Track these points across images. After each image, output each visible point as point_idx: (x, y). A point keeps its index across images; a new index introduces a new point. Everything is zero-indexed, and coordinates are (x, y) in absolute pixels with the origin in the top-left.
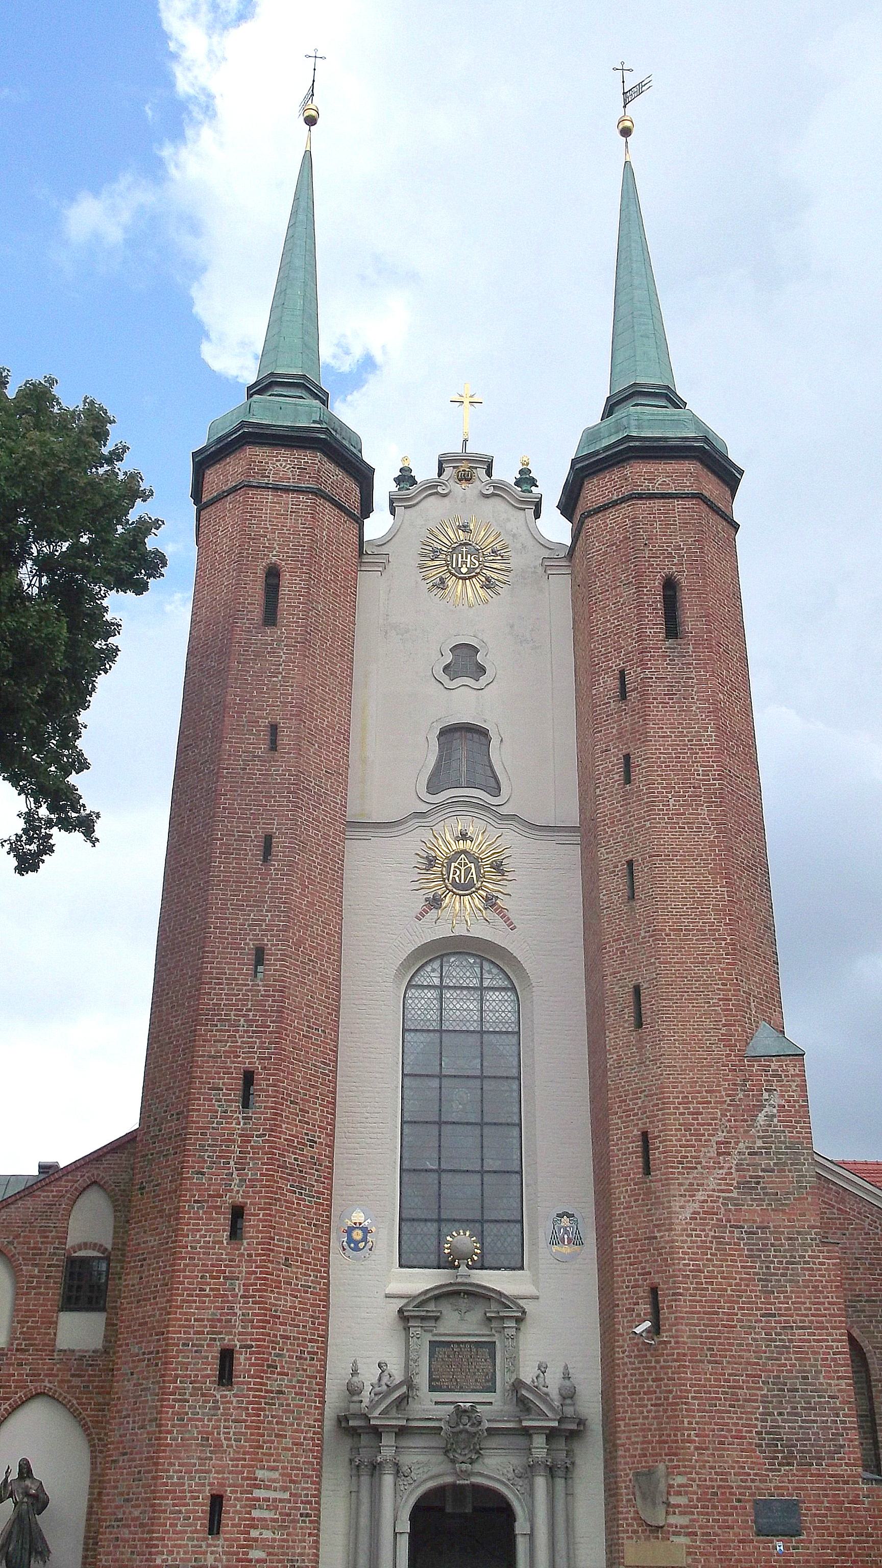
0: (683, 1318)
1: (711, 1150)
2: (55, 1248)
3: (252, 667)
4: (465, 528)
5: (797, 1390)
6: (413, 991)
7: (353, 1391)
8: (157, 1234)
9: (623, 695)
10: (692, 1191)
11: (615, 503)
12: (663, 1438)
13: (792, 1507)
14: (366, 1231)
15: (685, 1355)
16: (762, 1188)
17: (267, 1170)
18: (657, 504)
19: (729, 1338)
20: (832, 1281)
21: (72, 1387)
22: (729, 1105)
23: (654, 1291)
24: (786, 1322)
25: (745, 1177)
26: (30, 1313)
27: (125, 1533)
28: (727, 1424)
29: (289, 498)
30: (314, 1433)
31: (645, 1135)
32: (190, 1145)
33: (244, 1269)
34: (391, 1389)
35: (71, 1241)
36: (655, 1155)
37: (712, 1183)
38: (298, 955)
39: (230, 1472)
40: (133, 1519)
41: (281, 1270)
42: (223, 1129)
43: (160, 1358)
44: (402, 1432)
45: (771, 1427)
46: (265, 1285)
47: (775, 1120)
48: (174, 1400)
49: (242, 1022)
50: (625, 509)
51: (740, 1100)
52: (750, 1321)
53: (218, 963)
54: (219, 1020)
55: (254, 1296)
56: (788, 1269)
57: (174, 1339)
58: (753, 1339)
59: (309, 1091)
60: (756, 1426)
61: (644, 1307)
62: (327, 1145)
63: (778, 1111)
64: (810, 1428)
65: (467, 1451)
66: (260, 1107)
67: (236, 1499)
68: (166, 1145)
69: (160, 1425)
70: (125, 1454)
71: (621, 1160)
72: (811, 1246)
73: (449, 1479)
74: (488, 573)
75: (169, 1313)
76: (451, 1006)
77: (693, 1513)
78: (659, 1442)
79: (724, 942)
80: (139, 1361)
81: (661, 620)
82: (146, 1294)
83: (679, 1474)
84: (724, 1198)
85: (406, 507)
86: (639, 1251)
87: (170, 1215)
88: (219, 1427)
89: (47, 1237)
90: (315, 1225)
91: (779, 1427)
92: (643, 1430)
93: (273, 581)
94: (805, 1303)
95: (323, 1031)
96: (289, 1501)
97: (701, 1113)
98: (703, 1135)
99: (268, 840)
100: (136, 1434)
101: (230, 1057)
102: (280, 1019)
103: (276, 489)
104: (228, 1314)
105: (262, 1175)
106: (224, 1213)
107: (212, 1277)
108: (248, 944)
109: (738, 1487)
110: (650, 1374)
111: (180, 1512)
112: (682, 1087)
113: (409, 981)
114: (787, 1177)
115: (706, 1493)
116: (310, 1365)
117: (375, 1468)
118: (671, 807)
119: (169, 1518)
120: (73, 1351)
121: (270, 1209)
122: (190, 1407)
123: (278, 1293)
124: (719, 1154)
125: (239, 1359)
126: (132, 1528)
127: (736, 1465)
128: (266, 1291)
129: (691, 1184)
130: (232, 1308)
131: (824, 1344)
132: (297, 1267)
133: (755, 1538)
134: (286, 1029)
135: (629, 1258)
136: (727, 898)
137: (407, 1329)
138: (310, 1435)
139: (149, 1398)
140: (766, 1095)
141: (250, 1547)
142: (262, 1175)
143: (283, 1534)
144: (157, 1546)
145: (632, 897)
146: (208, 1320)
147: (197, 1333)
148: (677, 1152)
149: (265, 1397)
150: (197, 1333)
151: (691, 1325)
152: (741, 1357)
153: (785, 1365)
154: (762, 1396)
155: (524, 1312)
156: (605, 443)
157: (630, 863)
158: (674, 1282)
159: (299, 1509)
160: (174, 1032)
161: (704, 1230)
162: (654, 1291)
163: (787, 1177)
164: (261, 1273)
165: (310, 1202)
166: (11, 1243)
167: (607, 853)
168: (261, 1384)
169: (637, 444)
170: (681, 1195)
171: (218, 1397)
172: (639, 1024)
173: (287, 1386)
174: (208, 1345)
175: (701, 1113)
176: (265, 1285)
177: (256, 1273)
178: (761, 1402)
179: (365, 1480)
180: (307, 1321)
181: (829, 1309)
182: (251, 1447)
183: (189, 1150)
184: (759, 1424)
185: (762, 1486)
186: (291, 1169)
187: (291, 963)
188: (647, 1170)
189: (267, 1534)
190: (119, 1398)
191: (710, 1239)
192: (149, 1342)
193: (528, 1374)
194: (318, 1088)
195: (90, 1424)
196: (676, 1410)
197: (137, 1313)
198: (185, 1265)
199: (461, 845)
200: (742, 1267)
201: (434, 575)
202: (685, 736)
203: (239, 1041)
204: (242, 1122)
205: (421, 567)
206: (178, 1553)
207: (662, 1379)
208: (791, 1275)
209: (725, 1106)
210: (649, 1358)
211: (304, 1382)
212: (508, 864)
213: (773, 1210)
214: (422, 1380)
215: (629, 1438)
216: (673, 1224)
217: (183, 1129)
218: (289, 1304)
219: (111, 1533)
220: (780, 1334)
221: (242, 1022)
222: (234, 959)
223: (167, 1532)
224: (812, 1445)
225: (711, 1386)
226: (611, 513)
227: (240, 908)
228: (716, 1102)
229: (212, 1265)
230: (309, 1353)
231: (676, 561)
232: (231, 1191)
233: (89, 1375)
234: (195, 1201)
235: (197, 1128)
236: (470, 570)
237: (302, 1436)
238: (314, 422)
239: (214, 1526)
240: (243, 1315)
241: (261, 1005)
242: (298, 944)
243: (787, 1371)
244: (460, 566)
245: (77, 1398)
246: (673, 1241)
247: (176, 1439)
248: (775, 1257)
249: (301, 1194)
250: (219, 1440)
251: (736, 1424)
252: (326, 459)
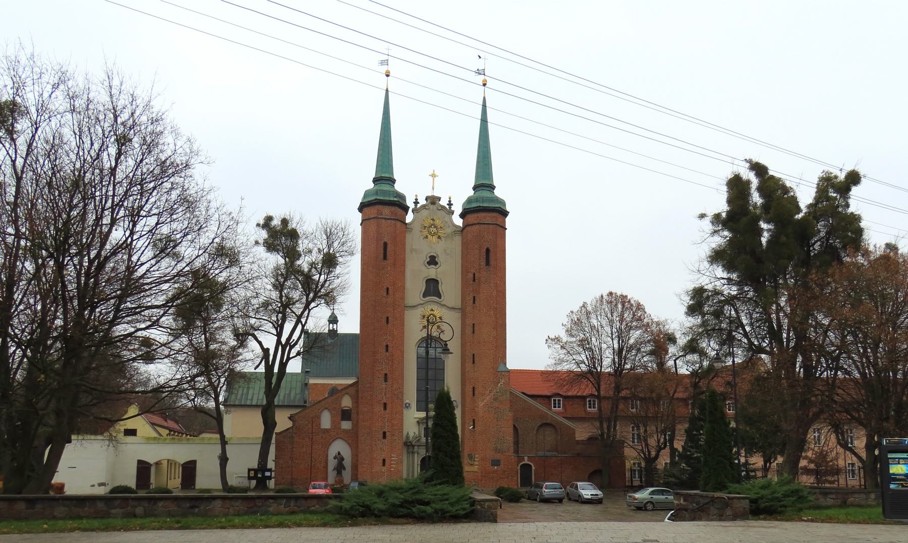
4: (433, 220)
7: (408, 437)
9: (474, 280)
10: (483, 400)
13: (499, 461)
14: (409, 404)
18: (486, 226)
23: (474, 420)
29: (389, 221)
31: (474, 388)
34: (416, 438)
36: (476, 392)
44: (418, 446)
50: (477, 226)
61: (472, 423)
99: (388, 318)
103: (385, 219)
117: (413, 453)
137: (419, 425)
145: (474, 332)
157: (474, 324)
162: (474, 420)
172: (474, 363)
179: (411, 455)
188: (474, 395)
199: (432, 312)
205: (421, 231)
236: (434, 233)
238: (395, 197)
239: (384, 465)
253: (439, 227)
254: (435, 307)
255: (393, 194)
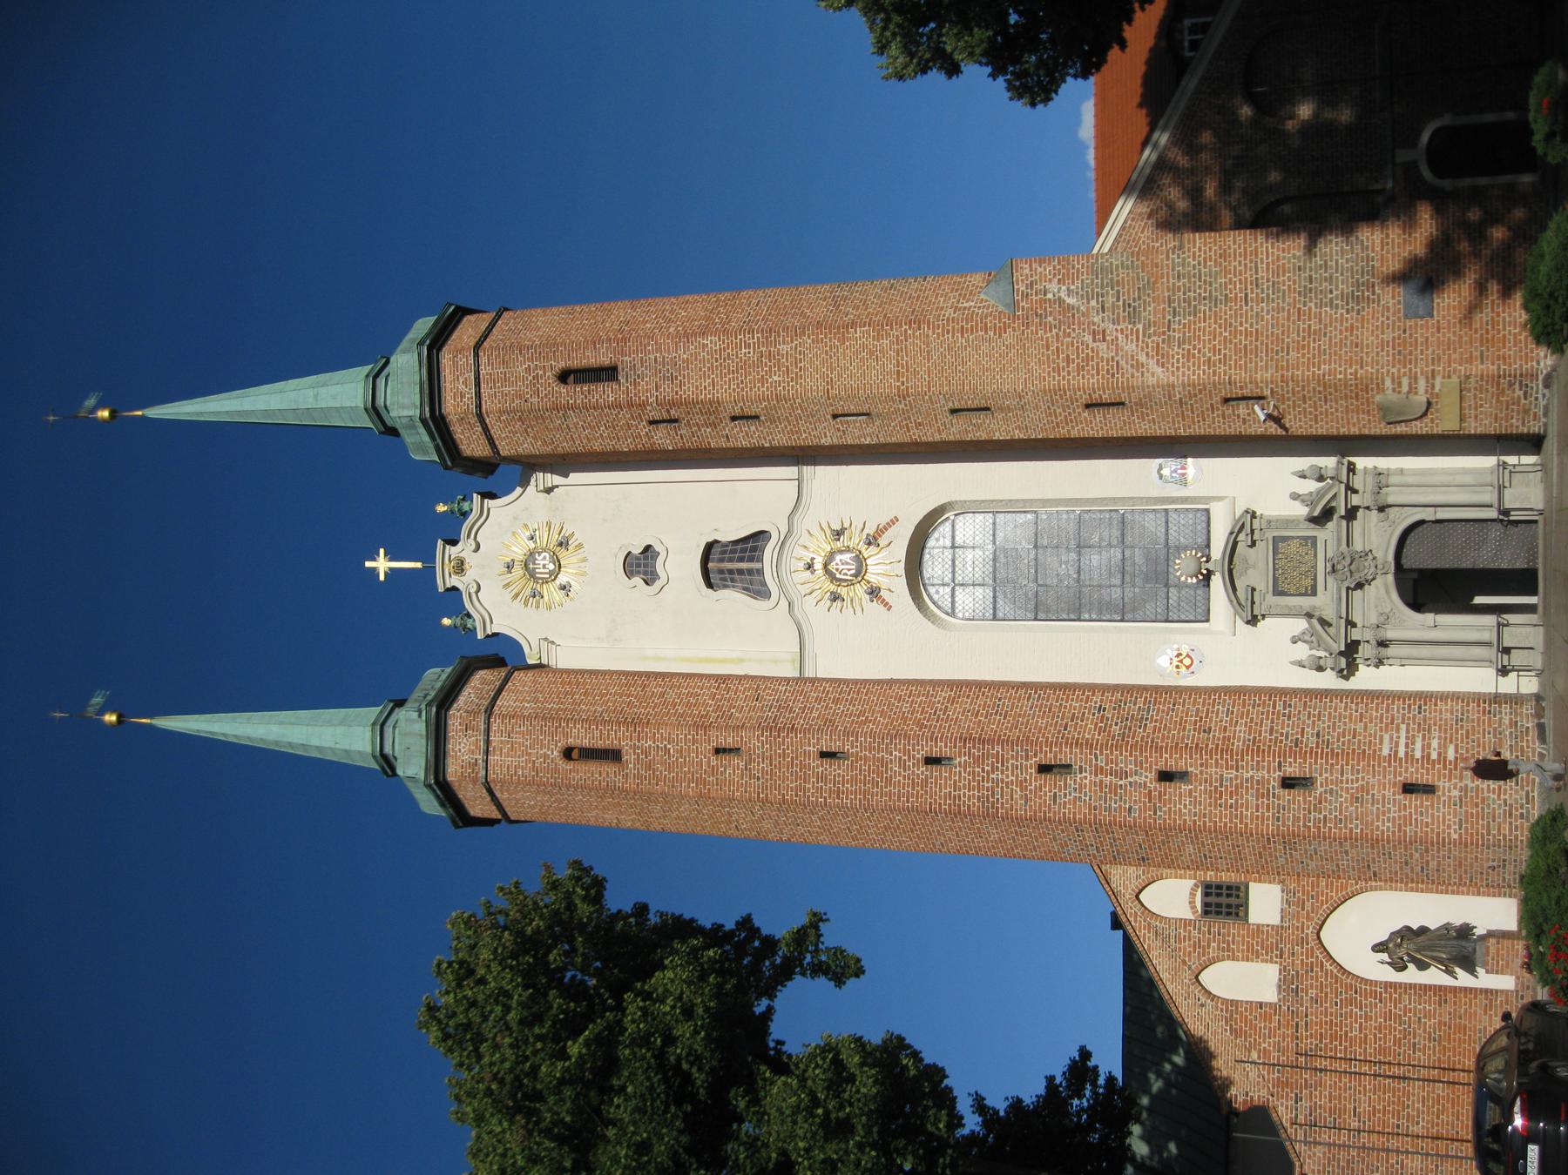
0: (1251, 377)
1: (1101, 347)
2: (1194, 929)
3: (661, 772)
5: (1310, 276)
6: (957, 611)
8: (1183, 845)
10: (1138, 366)
11: (486, 430)
12: (1354, 395)
15: (1282, 376)
16: (1134, 300)
17: (1126, 751)
19: (1267, 336)
20: (1215, 240)
21: (1313, 908)
22: (1060, 330)
23: (1226, 400)
24: (1252, 284)
25: (1124, 317)
26: (1250, 949)
27: (1432, 865)
28: (1341, 340)
30: (1352, 703)
31: (1088, 406)
32: (1105, 820)
33: (1214, 770)
35: (1189, 915)
36: (1106, 398)
37: (1130, 347)
38: (931, 725)
39: (1384, 777)
40: (1422, 857)
41: (1214, 736)
42: (1091, 791)
43: (1289, 840)
45: (1342, 301)
46: (1227, 751)
47: (1072, 287)
48: (1324, 828)
49: (994, 776)
51: (1055, 320)
52: (1252, 316)
53: (940, 798)
54: (993, 797)
55: (1237, 761)
56: (1205, 281)
57: (1273, 830)
58: (1268, 314)
59: (1054, 713)
60: (1342, 314)
61: (1242, 409)
62: (1103, 695)
63: (1064, 284)
64: (1342, 267)
65: (1366, 564)
66: (1071, 758)
67: (1406, 772)
68: (1105, 840)
69: (1346, 839)
70: (1369, 866)
71: (1111, 428)
72: (1184, 259)
73: (1390, 578)
74: (554, 542)
75: (1252, 835)
76: (971, 575)
77: (1416, 373)
78: (1357, 400)
79: (909, 332)
80: (1291, 857)
81: (600, 386)
82: (1235, 853)
83: (1383, 384)
84: (1144, 336)
85: (492, 622)
86: (1193, 413)
87: (1167, 836)
88: (1347, 788)
89: (1185, 937)
90: (1174, 705)
91: (1342, 293)
92: (1347, 413)
93: (575, 754)
94: (1235, 267)
95: (1000, 700)
96: (1408, 724)
97: (1068, 356)
98: (1087, 354)
100: (1352, 858)
101: (1026, 787)
102: (991, 741)
103: (487, 752)
104: (1252, 783)
105: (1131, 756)
106: (1165, 789)
107: (1221, 798)
108: (923, 772)
109: (1394, 332)
110: (1299, 406)
111: (1416, 820)
112: (1044, 372)
113: (948, 614)
114: (1123, 278)
115: (1399, 360)
116: (1295, 709)
118: (781, 379)
119: (1421, 829)
120: (1282, 909)
121: (1161, 747)
122: (1331, 814)
123: (1234, 738)
124: (1104, 340)
125: (1290, 773)
126: (1430, 858)
127: (1375, 333)
128: (1232, 750)
129: (1132, 366)
130: (1247, 780)
131: (1270, 251)
132: (1211, 720)
133: (1436, 318)
134: (1000, 736)
135: (1199, 421)
136: (867, 328)
137: (1264, 616)
138: (1354, 706)
139: (1322, 848)
140: (1050, 296)
141: (1445, 758)
142: (1131, 756)
143: (1435, 730)
144: (1444, 838)
146: (1257, 800)
147: (1268, 810)
148: (1103, 378)
149: (1322, 749)
150: (1268, 810)
151: (1256, 369)
152: (1283, 326)
153: (1289, 286)
154: (1316, 308)
155: (1247, 512)
156: (426, 438)
157: (835, 416)
158: (1220, 384)
159: (1414, 715)
160: (1003, 836)
161: (1173, 356)
162: (1226, 400)
163: (1123, 278)
164: (1217, 755)
165: (1154, 710)
166: (1190, 968)
167: (826, 437)
168: (1311, 752)
169: (427, 409)
170: (1143, 375)
171: (1322, 789)
172: (987, 409)
173: (1313, 729)
174: (1279, 800)
175: (1068, 356)
176: (1227, 751)
177: (1217, 760)
178: (1321, 308)
179: (1391, 651)
180: (1258, 711)
181: (1240, 244)
182: (1364, 761)
183: (1110, 821)
184: (1340, 311)
185: (1392, 310)
186: (1125, 728)
187: (939, 732)
189: (1435, 743)
190: (1323, 873)
191: (1181, 350)
192: (1275, 850)
193: (1301, 511)
194: (1051, 704)
195: (1344, 893)
196: (1330, 385)
197: (1251, 860)
198: (1210, 821)
199: (818, 566)
200: (1205, 322)
201: (558, 596)
202: (712, 364)
203: (1011, 778)
204: (1084, 774)
206: (1449, 820)
207: (1304, 396)
208: (1211, 277)
209: (1061, 333)
210: (1285, 406)
211: (1309, 713)
212: (837, 527)
213: (1153, 293)
214: (1306, 602)
215: (1354, 425)
216: (1168, 385)
217: (1091, 826)
218: (1243, 729)
219: (1433, 876)
220: (1262, 290)
221: (994, 776)
222: (936, 784)
223: (1432, 830)
224: (1357, 265)
225: (1308, 353)
226: (495, 432)
227: (889, 781)
228: (1057, 341)
229: (1211, 798)
230: (1285, 709)
231: (541, 372)
232: (1145, 783)
233: (1303, 895)
234: (1155, 814)
235: (1090, 814)
237: (1354, 713)
238: (420, 716)
239: (1429, 790)
240: (1252, 770)
241: (978, 760)
242: (922, 727)
243: (1295, 284)
244: (547, 571)
245: (1322, 905)
246: (1183, 384)
247: (1357, 825)
248: (1195, 292)
249: (1147, 719)
250: (1357, 788)
251: (1341, 331)
252: (455, 705)
253: (532, 545)
254: (798, 555)
255: (412, 721)
